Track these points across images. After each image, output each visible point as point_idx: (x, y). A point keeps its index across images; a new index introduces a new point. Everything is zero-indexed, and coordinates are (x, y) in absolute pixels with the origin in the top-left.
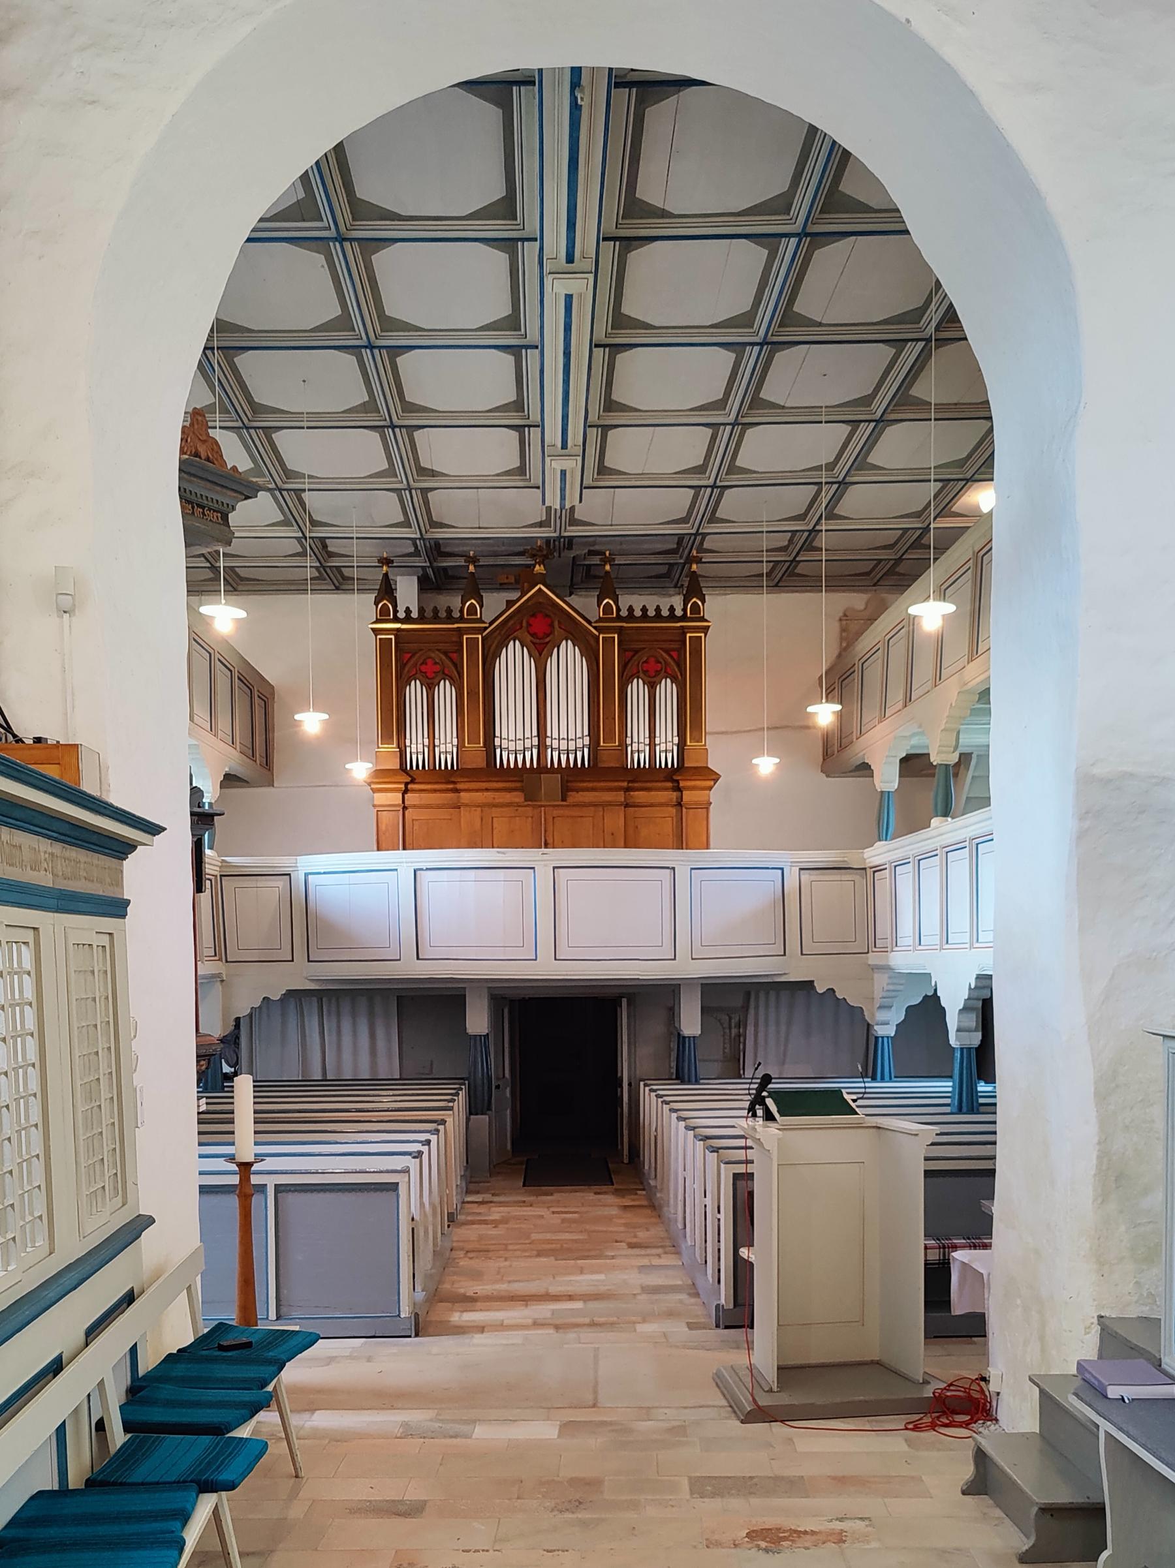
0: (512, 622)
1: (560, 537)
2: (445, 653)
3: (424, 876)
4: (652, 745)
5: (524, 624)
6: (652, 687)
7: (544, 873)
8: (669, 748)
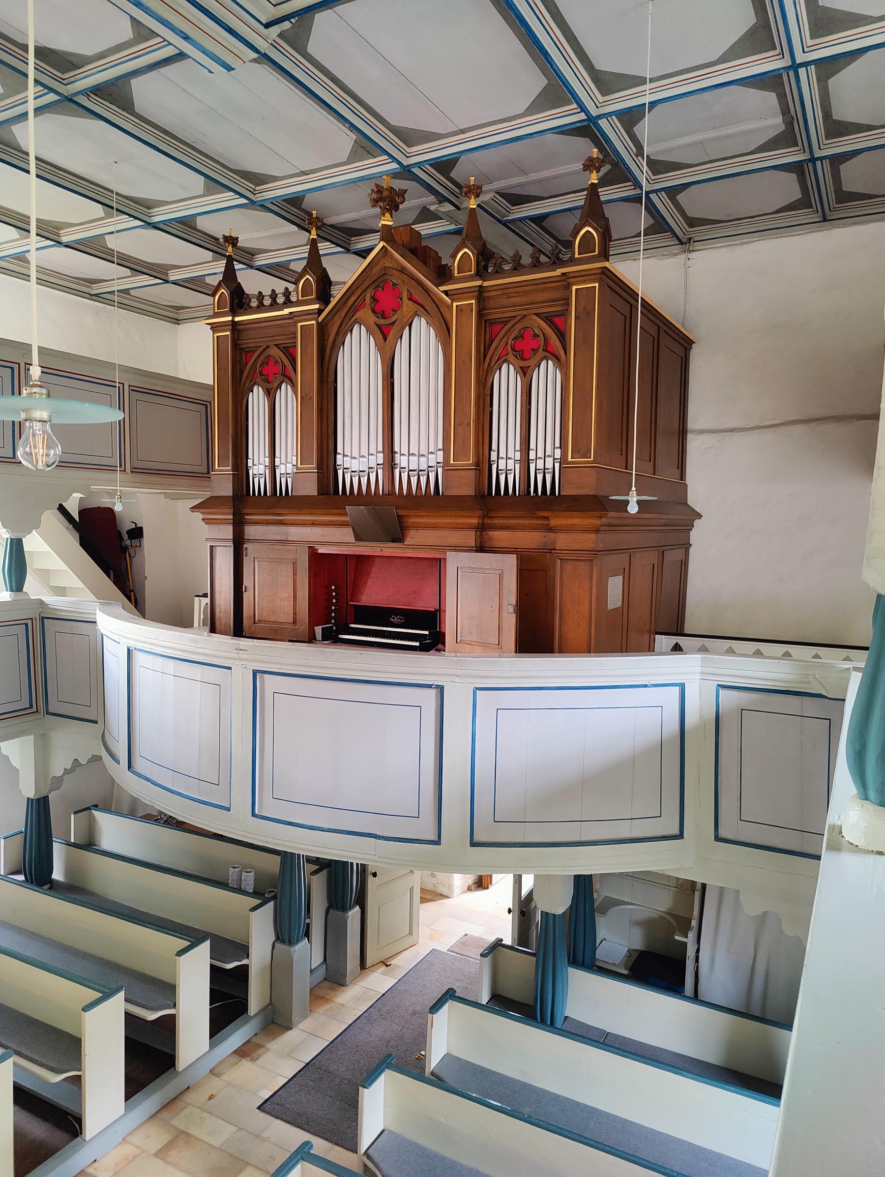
4: (525, 462)
8: (549, 465)
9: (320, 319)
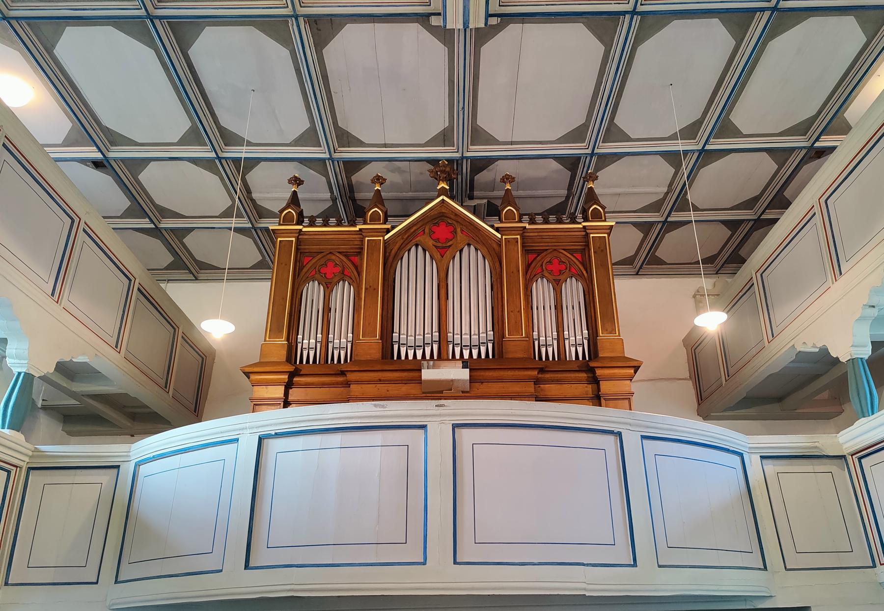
0: (414, 228)
1: (463, 158)
2: (346, 256)
3: (274, 446)
4: (561, 339)
5: (427, 230)
6: (557, 286)
7: (440, 435)
9: (386, 237)
